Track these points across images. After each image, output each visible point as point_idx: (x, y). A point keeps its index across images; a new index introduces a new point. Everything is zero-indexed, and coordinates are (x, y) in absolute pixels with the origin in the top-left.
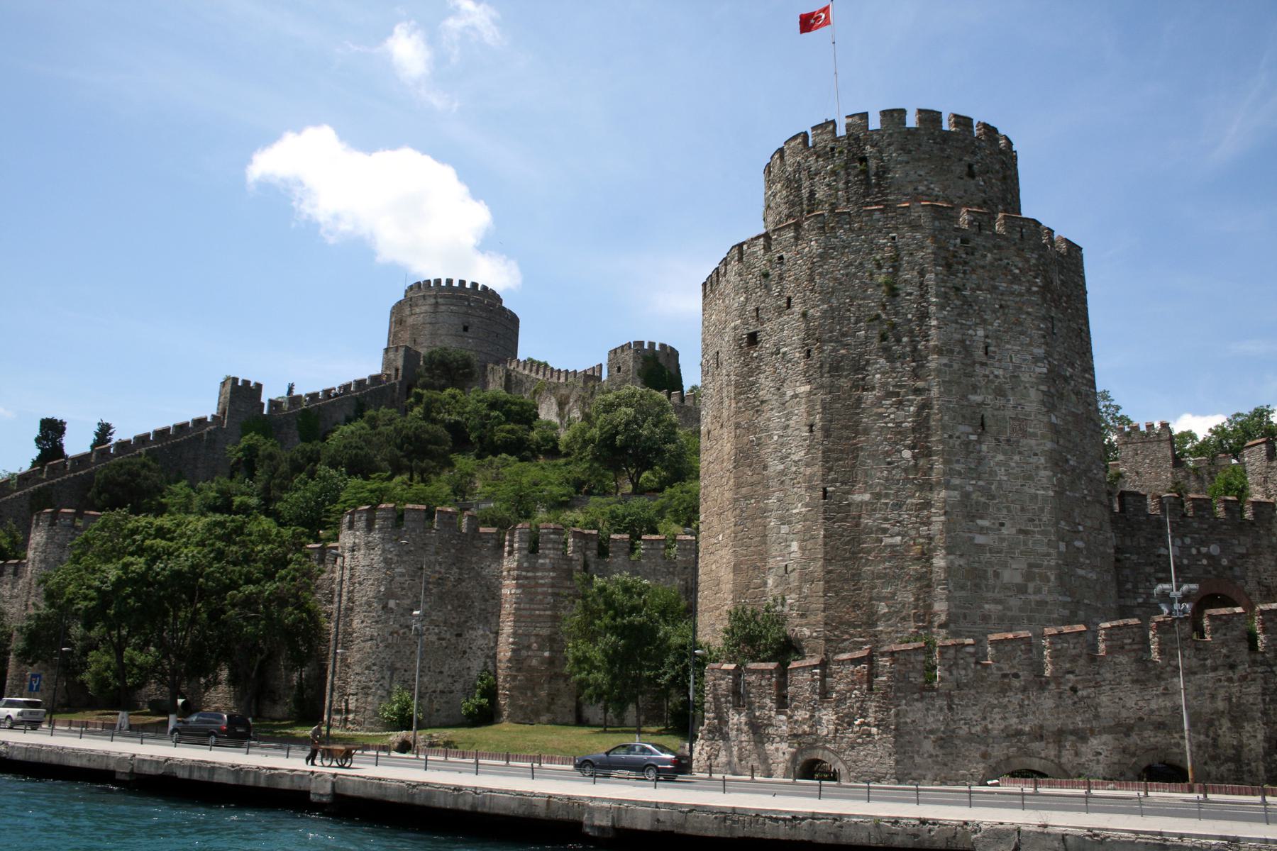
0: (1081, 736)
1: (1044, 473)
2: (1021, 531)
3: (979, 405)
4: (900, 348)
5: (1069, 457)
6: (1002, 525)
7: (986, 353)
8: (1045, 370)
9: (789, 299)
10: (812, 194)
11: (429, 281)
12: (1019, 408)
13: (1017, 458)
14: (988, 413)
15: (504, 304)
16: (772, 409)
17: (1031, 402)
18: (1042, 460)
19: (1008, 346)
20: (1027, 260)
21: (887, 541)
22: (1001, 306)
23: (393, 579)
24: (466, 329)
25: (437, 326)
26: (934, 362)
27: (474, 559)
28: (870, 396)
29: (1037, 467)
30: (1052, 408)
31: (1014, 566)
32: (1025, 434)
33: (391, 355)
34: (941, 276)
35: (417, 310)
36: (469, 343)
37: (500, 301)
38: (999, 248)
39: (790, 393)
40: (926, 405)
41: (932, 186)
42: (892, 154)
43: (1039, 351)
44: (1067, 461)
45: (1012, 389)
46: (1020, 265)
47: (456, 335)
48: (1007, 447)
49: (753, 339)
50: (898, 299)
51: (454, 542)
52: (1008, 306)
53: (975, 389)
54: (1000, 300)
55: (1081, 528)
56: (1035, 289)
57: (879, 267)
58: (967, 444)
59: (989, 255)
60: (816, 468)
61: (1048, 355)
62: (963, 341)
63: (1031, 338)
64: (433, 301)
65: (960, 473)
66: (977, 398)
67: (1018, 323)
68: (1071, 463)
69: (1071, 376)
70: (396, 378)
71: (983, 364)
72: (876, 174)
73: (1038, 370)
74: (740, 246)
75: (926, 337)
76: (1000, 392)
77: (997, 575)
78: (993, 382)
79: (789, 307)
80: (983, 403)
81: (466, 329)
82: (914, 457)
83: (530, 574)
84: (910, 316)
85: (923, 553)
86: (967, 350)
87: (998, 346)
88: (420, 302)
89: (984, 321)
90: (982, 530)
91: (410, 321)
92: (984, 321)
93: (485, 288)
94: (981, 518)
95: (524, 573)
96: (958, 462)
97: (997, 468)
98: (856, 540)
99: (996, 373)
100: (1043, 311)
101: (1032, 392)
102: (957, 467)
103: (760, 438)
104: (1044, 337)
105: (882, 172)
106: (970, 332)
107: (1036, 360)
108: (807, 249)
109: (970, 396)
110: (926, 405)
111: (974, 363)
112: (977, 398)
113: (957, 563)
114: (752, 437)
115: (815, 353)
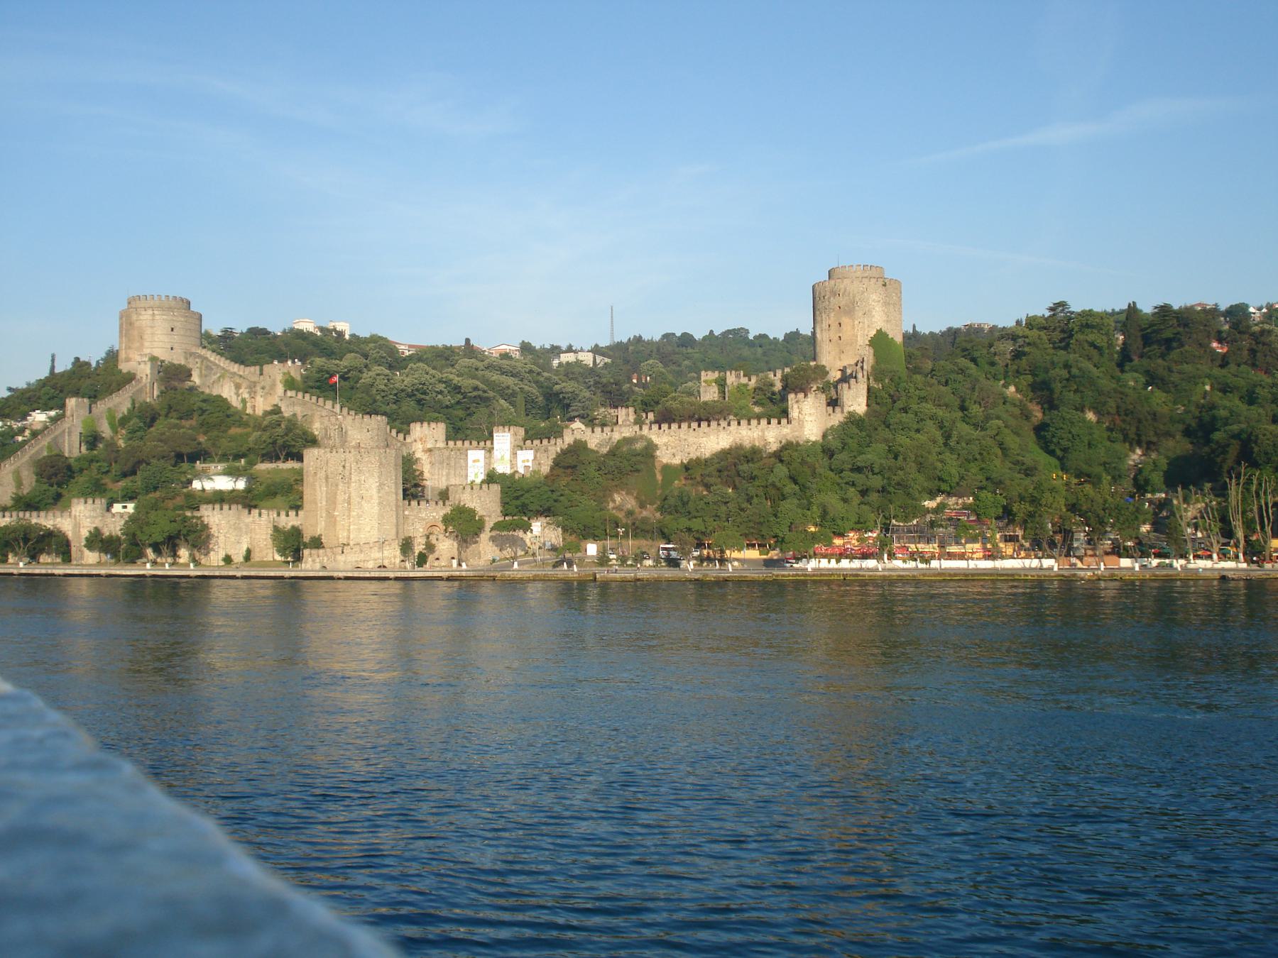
0: (368, 561)
24: (172, 330)
30: (379, 492)
35: (141, 318)
58: (359, 502)
64: (151, 312)
76: (367, 490)
81: (172, 330)
88: (143, 313)
91: (137, 324)
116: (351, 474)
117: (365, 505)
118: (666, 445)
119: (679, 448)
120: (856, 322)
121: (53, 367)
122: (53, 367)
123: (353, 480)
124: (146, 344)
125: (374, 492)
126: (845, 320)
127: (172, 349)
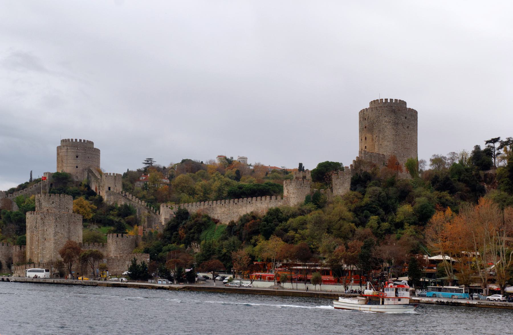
1: (53, 245)
11: (69, 139)
14: (46, 238)
18: (52, 243)
24: (77, 157)
25: (68, 156)
26: (40, 232)
28: (34, 236)
33: (45, 175)
35: (62, 151)
40: (39, 237)
47: (74, 159)
58: (43, 242)
64: (66, 148)
70: (47, 182)
75: (39, 229)
76: (48, 235)
81: (77, 157)
86: (44, 230)
88: (63, 148)
91: (61, 154)
98: (33, 252)
107: (53, 231)
110: (39, 237)
117: (47, 244)
118: (224, 213)
119: (229, 215)
120: (375, 136)
121: (31, 178)
122: (31, 178)
124: (64, 165)
125: (52, 236)
126: (369, 136)
127: (77, 167)
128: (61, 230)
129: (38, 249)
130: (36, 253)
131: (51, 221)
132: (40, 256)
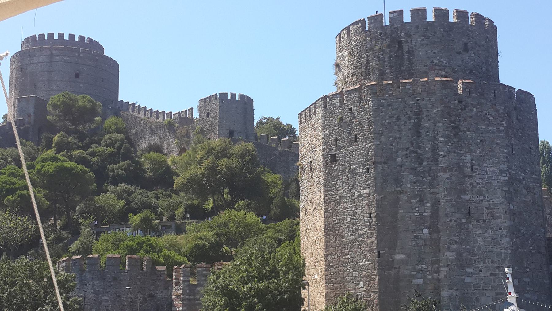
2: (491, 274)
3: (467, 201)
4: (421, 168)
5: (521, 228)
6: (481, 271)
7: (472, 170)
8: (507, 178)
9: (356, 136)
10: (368, 62)
12: (491, 201)
13: (489, 231)
15: (106, 54)
16: (347, 202)
17: (498, 198)
19: (485, 165)
20: (497, 111)
21: (415, 281)
22: (481, 141)
23: (100, 303)
24: (77, 76)
27: (152, 288)
28: (404, 197)
29: (501, 236)
30: (509, 199)
31: (487, 295)
32: (494, 217)
34: (446, 124)
35: (35, 60)
36: (81, 87)
37: (101, 49)
38: (481, 104)
39: (357, 193)
41: (442, 60)
42: (417, 40)
43: (503, 167)
44: (520, 231)
45: (487, 190)
46: (493, 114)
48: (484, 225)
49: (334, 159)
50: (421, 139)
51: (139, 277)
52: (485, 140)
53: (465, 192)
54: (481, 137)
55: (528, 270)
56: (502, 128)
57: (410, 118)
59: (475, 109)
60: (373, 239)
61: (509, 168)
62: (459, 163)
63: (499, 159)
64: (49, 53)
65: (456, 242)
66: (467, 197)
67: (492, 150)
68: (522, 231)
69: (523, 179)
71: (469, 176)
72: (408, 52)
73: (502, 178)
74: (325, 98)
75: (436, 161)
76: (480, 193)
77: (477, 300)
78: (476, 187)
79: (356, 141)
80: (470, 200)
81: (77, 76)
82: (430, 233)
83: (191, 297)
84: (427, 149)
85: (435, 289)
87: (479, 165)
89: (471, 151)
90: (469, 275)
92: (471, 151)
93: (90, 40)
94: (469, 267)
95: (187, 297)
96: (455, 235)
97: (477, 238)
99: (477, 181)
100: (506, 142)
101: (499, 191)
102: (455, 238)
103: (340, 220)
104: (507, 157)
105: (411, 52)
106: (463, 157)
107: (502, 172)
108: (366, 106)
109: (462, 196)
110: (436, 203)
111: (465, 176)
112: (467, 197)
113: (455, 294)
114: (335, 218)
115: (372, 171)
116: (435, 149)
123: (443, 162)
128: (525, 172)
129: (437, 261)
130: (421, 281)
131: (491, 123)
132: (450, 298)
